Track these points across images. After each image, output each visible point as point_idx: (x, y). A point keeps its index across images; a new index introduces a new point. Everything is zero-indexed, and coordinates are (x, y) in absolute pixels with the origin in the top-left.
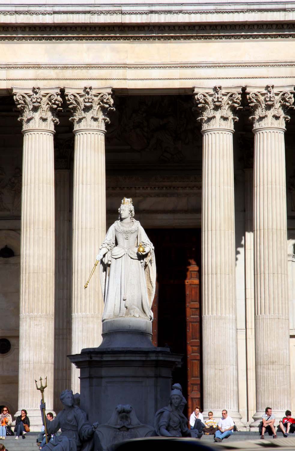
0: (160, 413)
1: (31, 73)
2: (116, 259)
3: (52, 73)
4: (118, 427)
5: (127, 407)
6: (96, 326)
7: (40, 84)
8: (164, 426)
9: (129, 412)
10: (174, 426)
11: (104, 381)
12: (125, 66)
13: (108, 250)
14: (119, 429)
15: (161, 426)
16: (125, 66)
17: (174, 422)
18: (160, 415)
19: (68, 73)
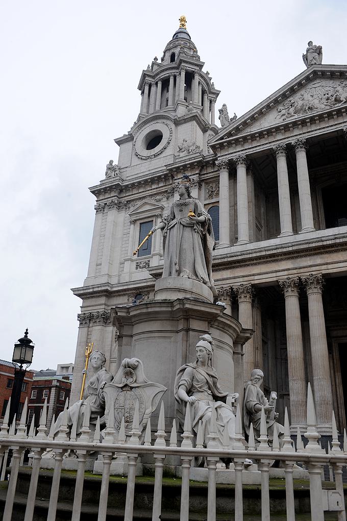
0: (181, 371)
1: (286, 273)
2: (170, 229)
3: (295, 271)
4: (121, 385)
5: (133, 361)
6: (325, 383)
7: (290, 276)
8: (183, 386)
9: (135, 368)
10: (197, 386)
11: (135, 338)
12: (327, 264)
13: (165, 225)
14: (122, 388)
15: (180, 385)
16: (327, 264)
17: (198, 381)
18: (181, 373)
19: (302, 270)
